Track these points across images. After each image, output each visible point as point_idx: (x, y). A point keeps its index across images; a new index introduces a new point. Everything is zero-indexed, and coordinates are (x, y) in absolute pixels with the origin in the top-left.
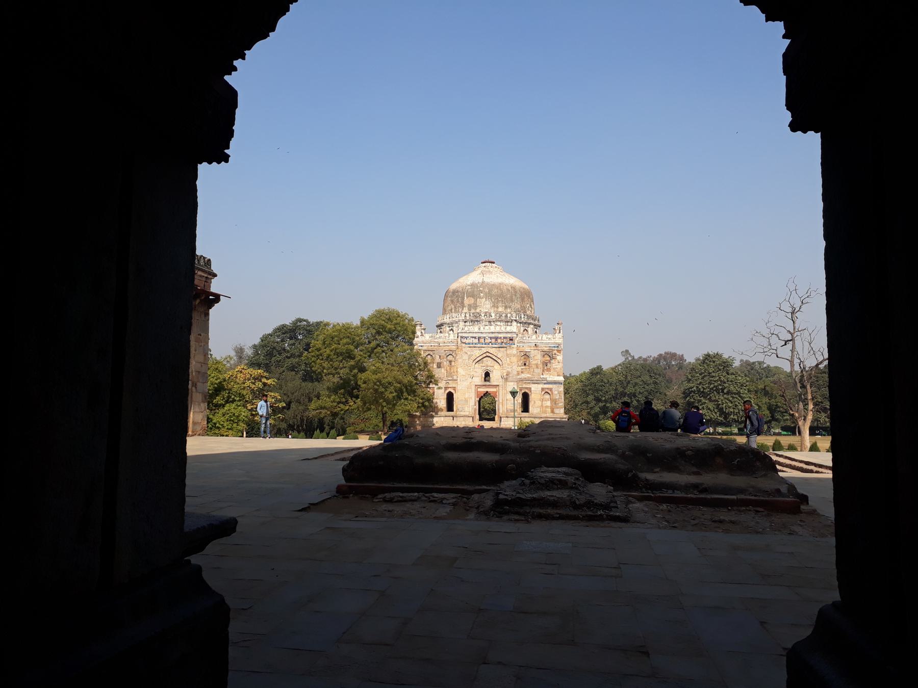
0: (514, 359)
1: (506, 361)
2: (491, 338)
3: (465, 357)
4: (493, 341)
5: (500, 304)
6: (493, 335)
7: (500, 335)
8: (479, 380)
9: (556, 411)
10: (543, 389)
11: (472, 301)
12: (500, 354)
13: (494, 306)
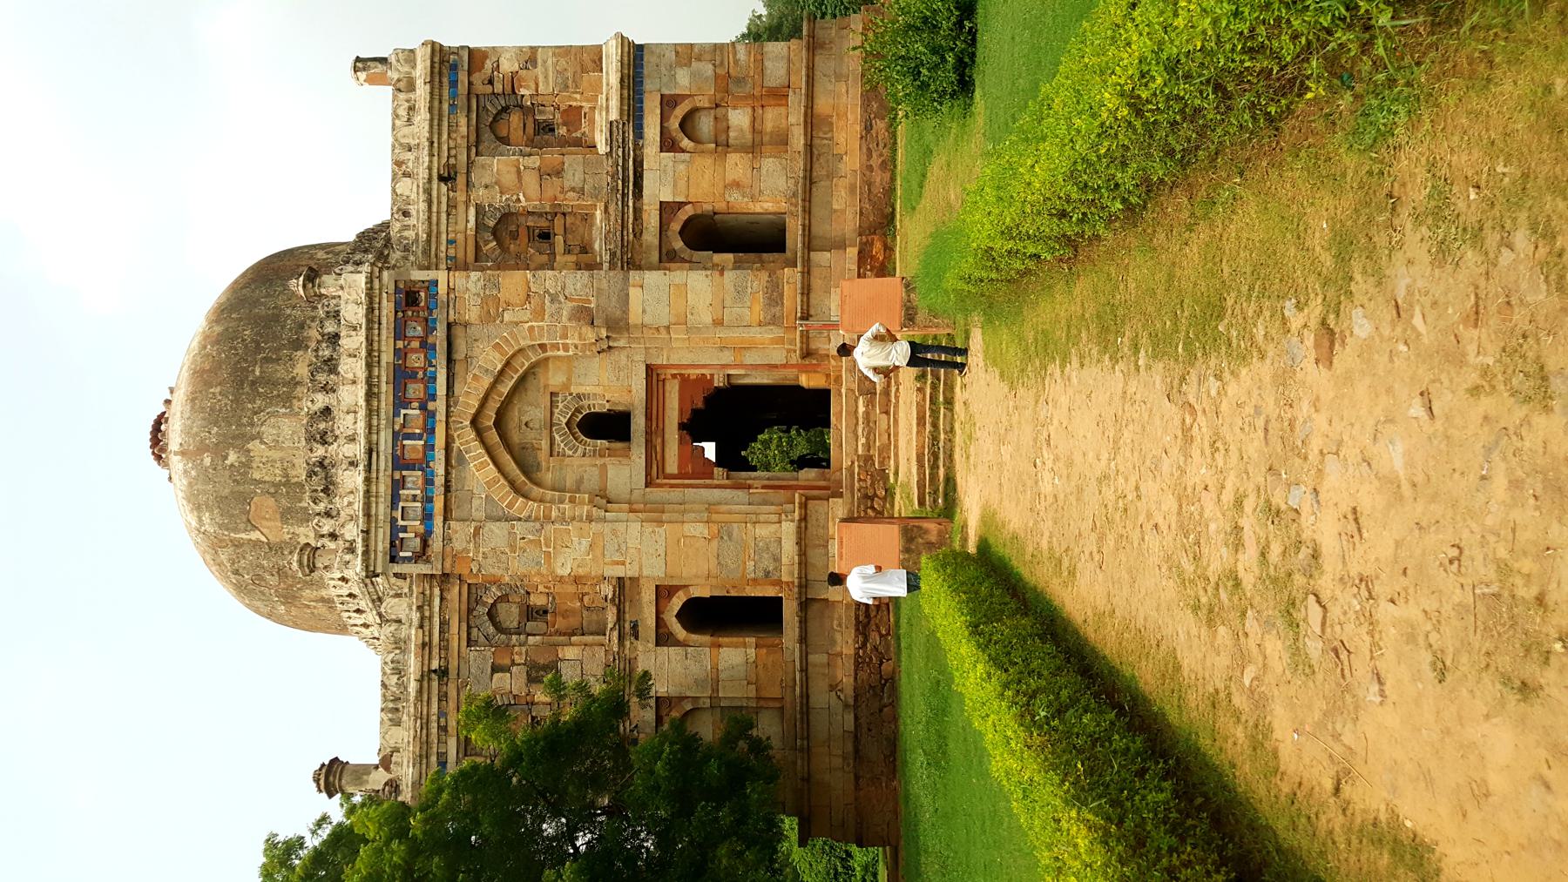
0: (513, 282)
1: (522, 327)
2: (401, 402)
3: (496, 534)
4: (415, 390)
5: (281, 372)
6: (385, 389)
7: (387, 357)
8: (624, 470)
9: (775, 72)
10: (668, 144)
11: (265, 505)
12: (485, 358)
13: (287, 400)
